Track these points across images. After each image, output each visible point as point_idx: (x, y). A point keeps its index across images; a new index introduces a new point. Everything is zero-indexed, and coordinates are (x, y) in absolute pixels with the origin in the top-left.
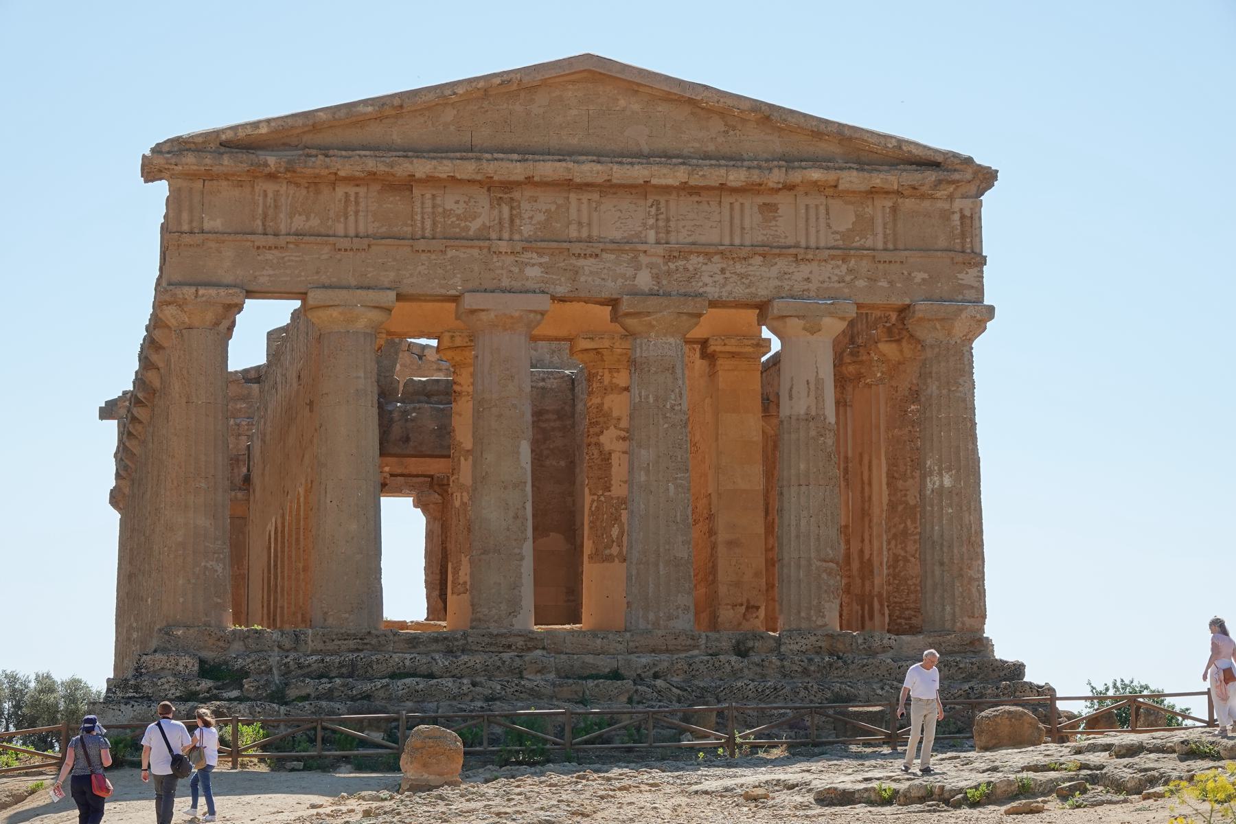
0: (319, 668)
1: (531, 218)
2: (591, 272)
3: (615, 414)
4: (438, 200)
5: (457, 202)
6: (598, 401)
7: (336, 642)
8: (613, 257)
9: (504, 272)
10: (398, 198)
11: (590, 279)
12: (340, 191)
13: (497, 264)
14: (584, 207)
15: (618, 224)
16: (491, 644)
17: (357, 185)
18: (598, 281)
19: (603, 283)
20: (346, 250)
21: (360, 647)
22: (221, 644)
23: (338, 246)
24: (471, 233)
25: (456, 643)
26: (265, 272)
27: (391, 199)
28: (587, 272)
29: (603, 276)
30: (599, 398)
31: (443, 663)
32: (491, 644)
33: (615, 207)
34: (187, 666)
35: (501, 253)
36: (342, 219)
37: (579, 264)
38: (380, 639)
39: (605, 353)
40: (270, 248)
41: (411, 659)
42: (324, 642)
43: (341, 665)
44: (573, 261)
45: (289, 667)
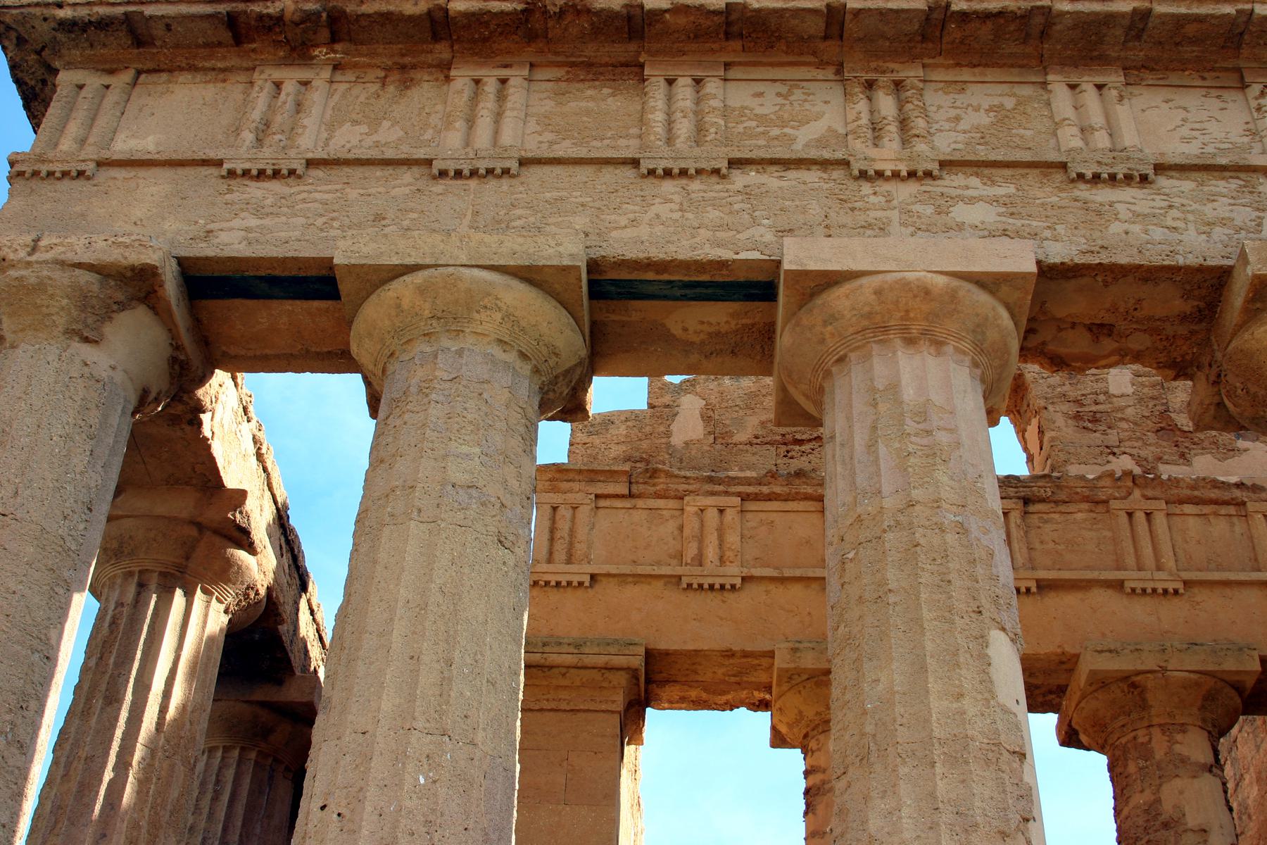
2: (1137, 215)
3: (1192, 821)
5: (760, 95)
6: (1147, 796)
8: (1187, 185)
10: (606, 91)
11: (1136, 228)
12: (462, 77)
13: (873, 199)
14: (1090, 95)
15: (1185, 131)
18: (1158, 233)
19: (1176, 236)
23: (438, 166)
24: (798, 146)
26: (237, 223)
27: (589, 92)
29: (1170, 223)
30: (1148, 792)
35: (880, 174)
36: (460, 124)
37: (1099, 199)
39: (1150, 684)
40: (261, 174)
44: (1083, 191)
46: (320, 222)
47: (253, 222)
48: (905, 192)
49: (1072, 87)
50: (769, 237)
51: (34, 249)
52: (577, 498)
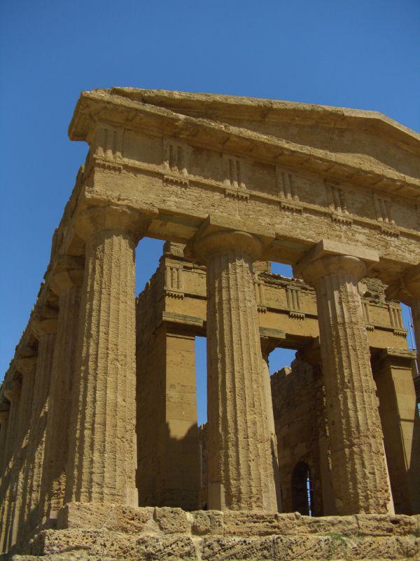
0: (242, 549)
1: (353, 204)
4: (294, 178)
5: (305, 184)
7: (248, 524)
9: (342, 234)
10: (265, 172)
11: (395, 249)
13: (338, 228)
16: (378, 528)
17: (239, 157)
18: (400, 252)
20: (233, 195)
21: (270, 530)
22: (135, 523)
25: (350, 527)
28: (393, 245)
31: (352, 544)
32: (378, 528)
33: (400, 209)
34: (105, 546)
38: (286, 522)
41: (325, 541)
42: (237, 524)
43: (264, 547)
45: (212, 549)
46: (196, 203)
47: (177, 200)
48: (344, 228)
49: (379, 200)
50: (314, 235)
51: (119, 200)
52: (178, 266)
